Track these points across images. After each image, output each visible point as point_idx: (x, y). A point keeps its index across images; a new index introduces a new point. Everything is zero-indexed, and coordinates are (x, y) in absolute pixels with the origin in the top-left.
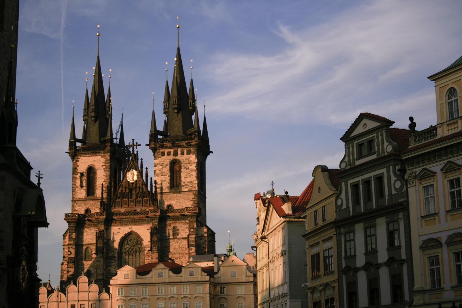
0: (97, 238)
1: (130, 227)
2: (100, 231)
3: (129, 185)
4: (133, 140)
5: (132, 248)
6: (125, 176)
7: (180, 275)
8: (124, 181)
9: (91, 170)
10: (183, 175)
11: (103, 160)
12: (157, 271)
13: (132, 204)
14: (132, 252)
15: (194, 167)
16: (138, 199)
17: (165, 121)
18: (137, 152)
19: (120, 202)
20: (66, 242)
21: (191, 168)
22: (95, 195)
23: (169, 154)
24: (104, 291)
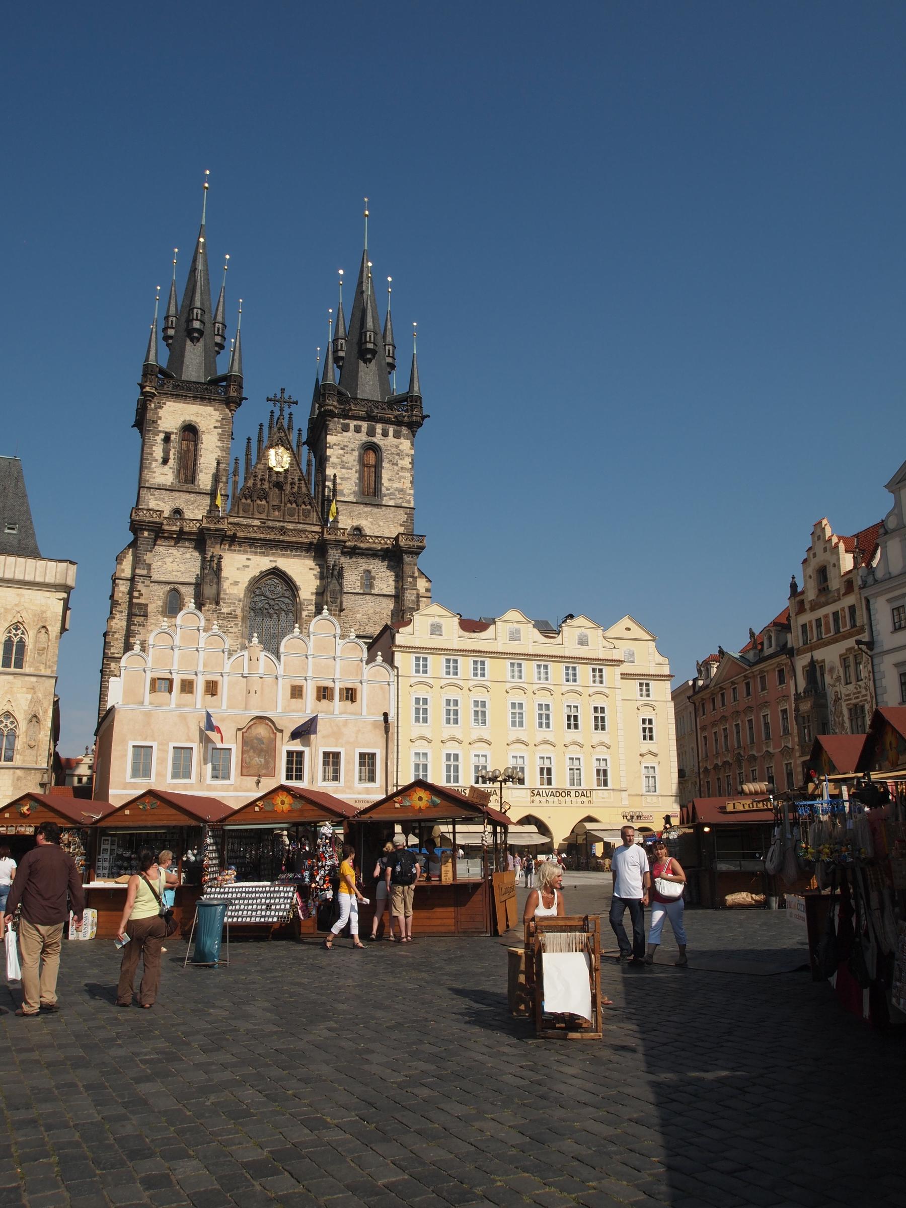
0: (203, 568)
1: (272, 558)
2: (212, 557)
3: (270, 476)
4: (283, 390)
5: (271, 602)
6: (262, 456)
7: (559, 639)
8: (260, 466)
9: (190, 431)
10: (385, 475)
11: (217, 415)
12: (509, 625)
13: (277, 513)
14: (271, 611)
15: (406, 462)
16: (289, 505)
17: (317, 380)
18: (291, 414)
19: (249, 505)
20: (123, 571)
21: (401, 462)
22: (196, 483)
23: (358, 430)
24: (379, 658)
